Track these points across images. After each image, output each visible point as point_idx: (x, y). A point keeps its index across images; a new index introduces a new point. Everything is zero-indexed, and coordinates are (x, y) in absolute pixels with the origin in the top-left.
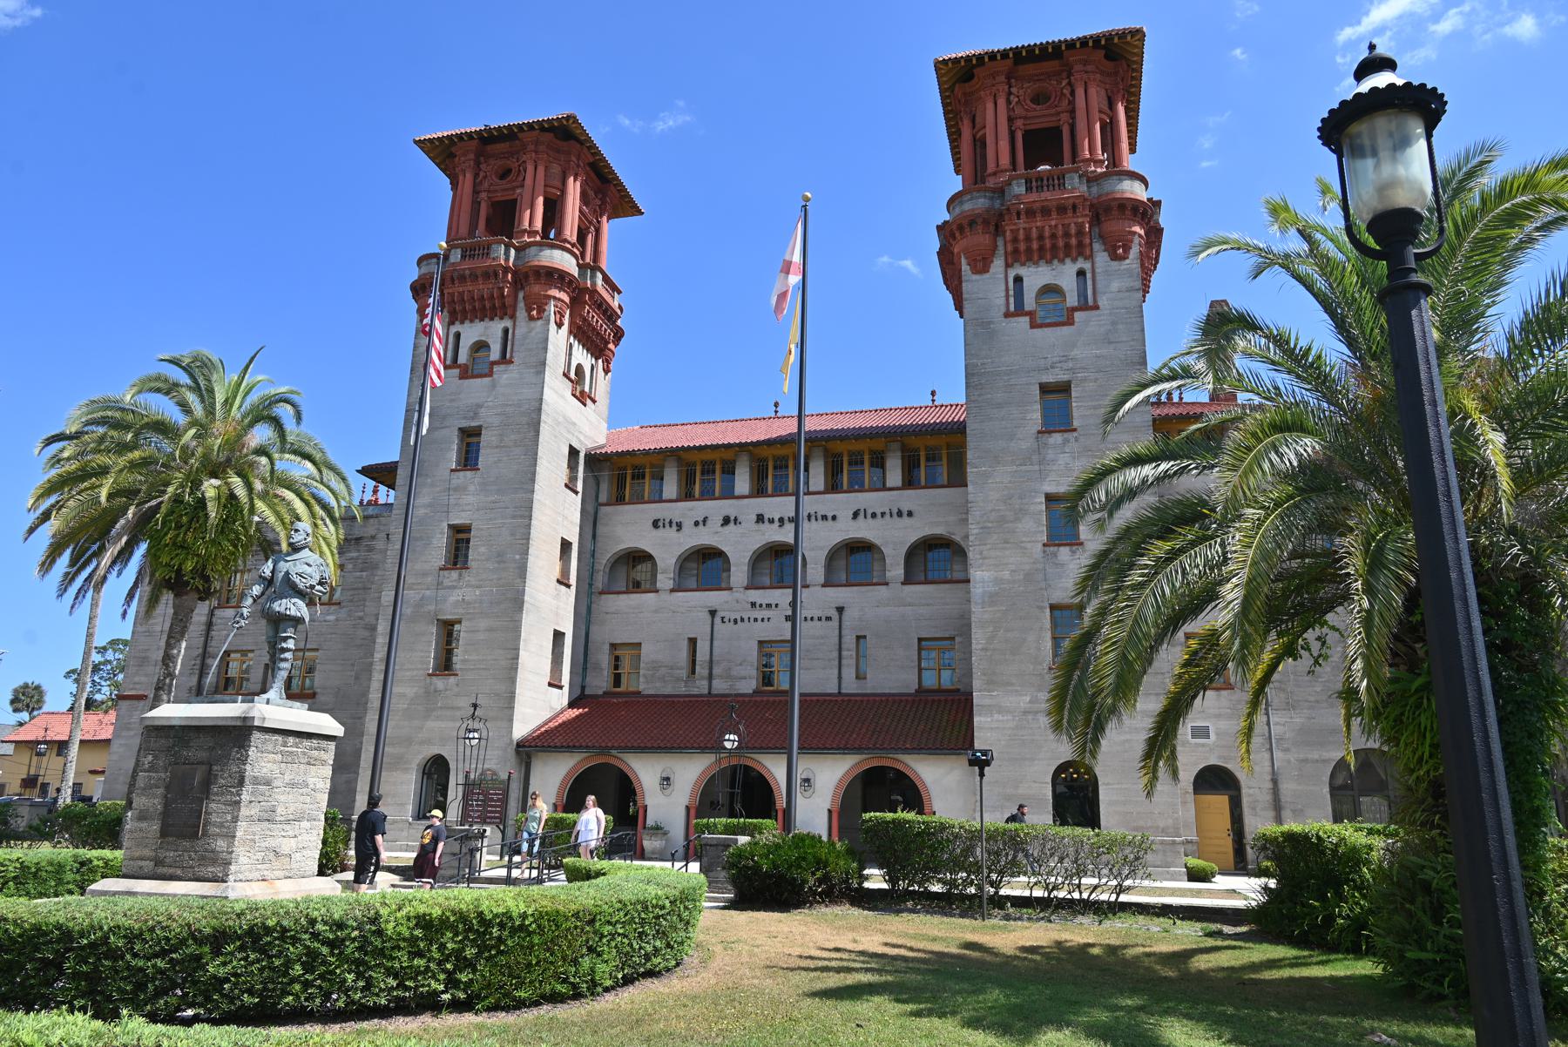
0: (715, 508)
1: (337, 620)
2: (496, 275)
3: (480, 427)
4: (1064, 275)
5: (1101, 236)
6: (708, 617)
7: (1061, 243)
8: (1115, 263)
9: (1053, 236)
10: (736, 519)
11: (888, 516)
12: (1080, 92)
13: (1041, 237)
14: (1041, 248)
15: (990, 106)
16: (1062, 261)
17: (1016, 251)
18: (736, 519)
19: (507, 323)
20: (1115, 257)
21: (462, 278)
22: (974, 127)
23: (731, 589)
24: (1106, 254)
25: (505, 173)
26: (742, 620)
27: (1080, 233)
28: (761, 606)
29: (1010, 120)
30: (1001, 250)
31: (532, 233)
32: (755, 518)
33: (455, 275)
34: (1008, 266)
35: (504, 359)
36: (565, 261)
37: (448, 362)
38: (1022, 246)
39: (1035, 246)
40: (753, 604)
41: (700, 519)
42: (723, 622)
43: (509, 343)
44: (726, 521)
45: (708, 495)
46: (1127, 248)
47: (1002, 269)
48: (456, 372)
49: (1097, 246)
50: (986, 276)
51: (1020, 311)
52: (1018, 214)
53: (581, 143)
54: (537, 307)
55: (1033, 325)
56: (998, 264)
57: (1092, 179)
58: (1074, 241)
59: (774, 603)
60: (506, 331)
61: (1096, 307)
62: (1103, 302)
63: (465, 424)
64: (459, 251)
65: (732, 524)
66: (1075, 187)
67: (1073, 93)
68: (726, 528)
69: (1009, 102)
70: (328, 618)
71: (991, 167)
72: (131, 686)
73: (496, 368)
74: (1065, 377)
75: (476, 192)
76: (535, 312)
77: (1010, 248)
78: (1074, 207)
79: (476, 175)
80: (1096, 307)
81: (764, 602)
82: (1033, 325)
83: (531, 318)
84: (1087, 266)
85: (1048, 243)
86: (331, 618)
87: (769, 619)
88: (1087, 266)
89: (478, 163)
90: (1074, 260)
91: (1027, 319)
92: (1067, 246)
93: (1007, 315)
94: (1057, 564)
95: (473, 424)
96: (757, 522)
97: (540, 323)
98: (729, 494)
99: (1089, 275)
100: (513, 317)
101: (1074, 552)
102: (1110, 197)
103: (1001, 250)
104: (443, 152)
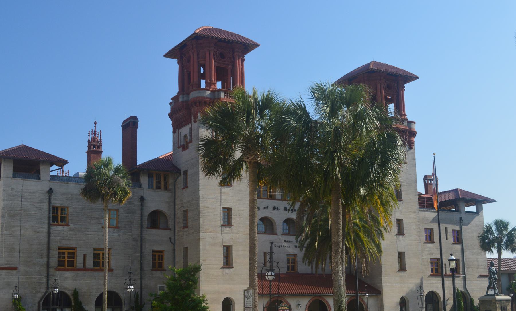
0: (271, 203)
1: (119, 235)
6: (270, 245)
18: (277, 208)
23: (276, 234)
26: (281, 246)
28: (287, 241)
40: (285, 241)
41: (266, 206)
42: (275, 247)
59: (291, 241)
65: (276, 210)
70: (114, 234)
72: (6, 263)
81: (288, 240)
86: (116, 234)
87: (290, 246)
94: (399, 240)
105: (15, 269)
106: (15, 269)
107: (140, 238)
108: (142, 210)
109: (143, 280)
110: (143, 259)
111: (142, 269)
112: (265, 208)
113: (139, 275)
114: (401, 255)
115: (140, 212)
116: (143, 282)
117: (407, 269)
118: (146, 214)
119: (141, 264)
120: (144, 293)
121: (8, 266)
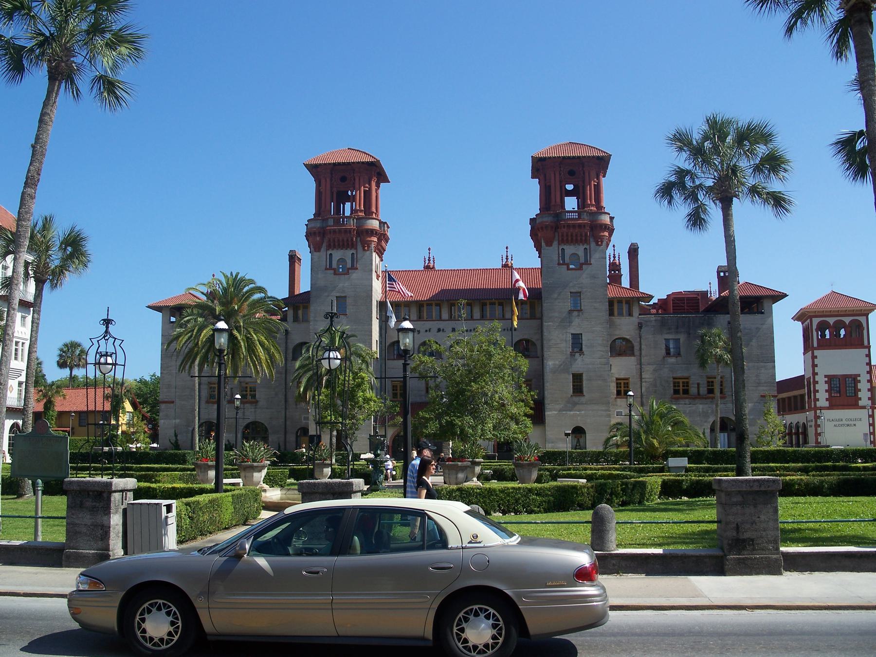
2: (350, 232)
3: (345, 297)
4: (580, 250)
5: (593, 235)
7: (579, 238)
8: (598, 247)
9: (576, 235)
10: (443, 330)
11: (506, 330)
12: (587, 174)
13: (572, 235)
14: (572, 239)
15: (553, 175)
16: (579, 245)
17: (563, 239)
18: (443, 330)
19: (353, 251)
20: (597, 245)
21: (334, 231)
22: (545, 180)
24: (594, 243)
25: (343, 179)
27: (586, 234)
29: (561, 182)
30: (557, 237)
31: (361, 211)
32: (451, 329)
33: (332, 231)
34: (559, 244)
35: (353, 268)
36: (374, 224)
37: (328, 267)
38: (565, 239)
39: (570, 239)
41: (428, 329)
43: (355, 260)
44: (439, 330)
45: (430, 319)
46: (602, 242)
47: (557, 246)
48: (332, 271)
49: (591, 240)
50: (551, 248)
51: (564, 264)
52: (564, 226)
53: (376, 166)
54: (366, 245)
55: (568, 269)
56: (555, 243)
57: (592, 214)
58: (584, 238)
60: (353, 254)
61: (591, 264)
62: (593, 261)
63: (338, 295)
64: (332, 220)
65: (441, 332)
66: (586, 219)
67: (584, 173)
68: (439, 333)
69: (560, 174)
71: (553, 203)
73: (350, 271)
74: (580, 290)
75: (331, 187)
76: (366, 248)
77: (560, 239)
78: (584, 226)
79: (331, 180)
80: (591, 264)
82: (568, 269)
83: (364, 250)
84: (588, 247)
85: (574, 238)
88: (588, 247)
89: (332, 174)
90: (583, 245)
91: (566, 266)
92: (581, 239)
93: (559, 264)
95: (342, 295)
96: (452, 331)
97: (368, 252)
98: (440, 319)
99: (588, 251)
100: (356, 249)
101: (580, 355)
102: (599, 222)
103: (557, 237)
104: (314, 169)
105: (173, 402)
106: (173, 402)
107: (284, 371)
108: (286, 343)
109: (287, 411)
110: (287, 391)
111: (286, 401)
112: (426, 331)
113: (284, 407)
114: (577, 379)
115: (284, 345)
116: (287, 413)
117: (585, 393)
118: (291, 347)
119: (286, 395)
120: (288, 423)
121: (166, 400)
